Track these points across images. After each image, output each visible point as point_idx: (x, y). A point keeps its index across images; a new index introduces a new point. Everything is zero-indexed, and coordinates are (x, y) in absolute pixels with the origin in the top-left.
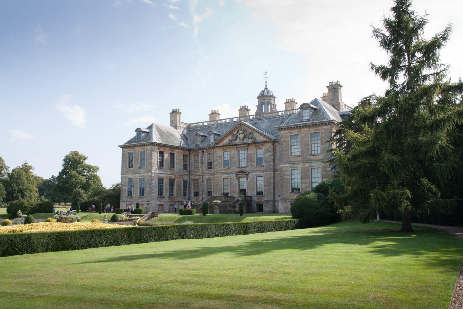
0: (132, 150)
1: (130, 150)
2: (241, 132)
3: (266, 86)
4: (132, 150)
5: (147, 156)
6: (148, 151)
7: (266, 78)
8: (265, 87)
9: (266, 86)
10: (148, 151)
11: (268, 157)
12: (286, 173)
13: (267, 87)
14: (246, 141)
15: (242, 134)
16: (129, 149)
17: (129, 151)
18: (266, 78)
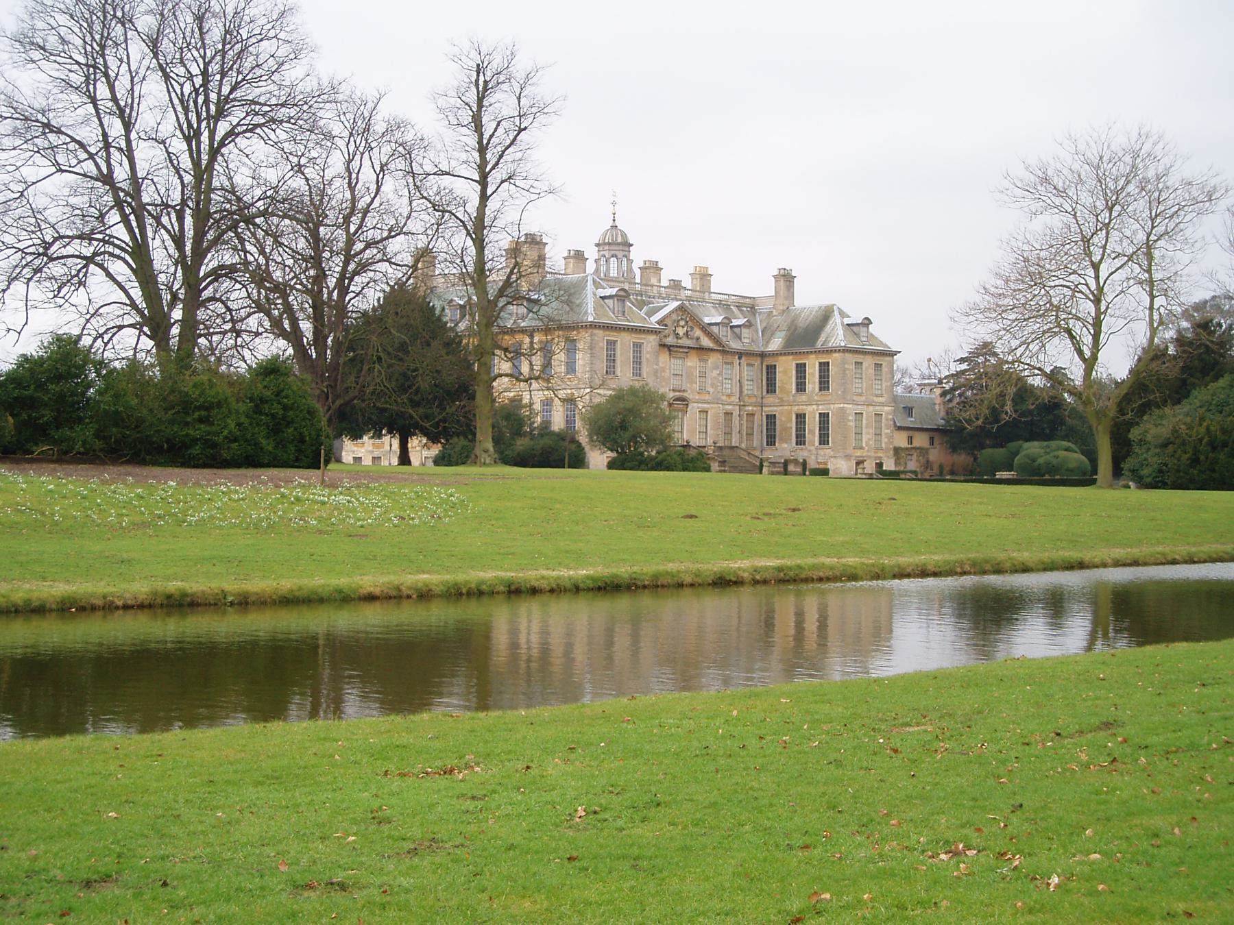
0: (613, 336)
1: (609, 336)
2: (682, 323)
3: (614, 220)
4: (613, 336)
5: (648, 356)
6: (649, 345)
7: (614, 204)
8: (611, 223)
9: (614, 220)
10: (649, 345)
11: (715, 377)
12: (850, 418)
13: (617, 223)
14: (684, 342)
15: (683, 327)
16: (607, 333)
17: (609, 338)
18: (614, 204)
